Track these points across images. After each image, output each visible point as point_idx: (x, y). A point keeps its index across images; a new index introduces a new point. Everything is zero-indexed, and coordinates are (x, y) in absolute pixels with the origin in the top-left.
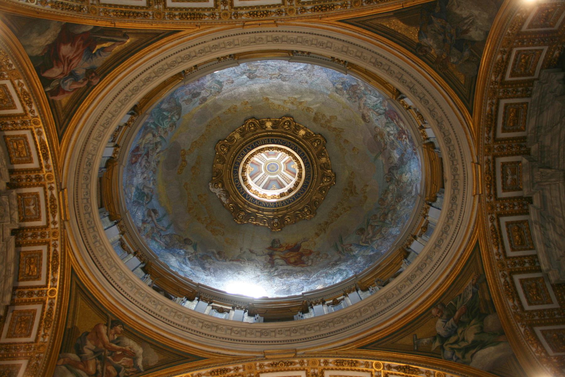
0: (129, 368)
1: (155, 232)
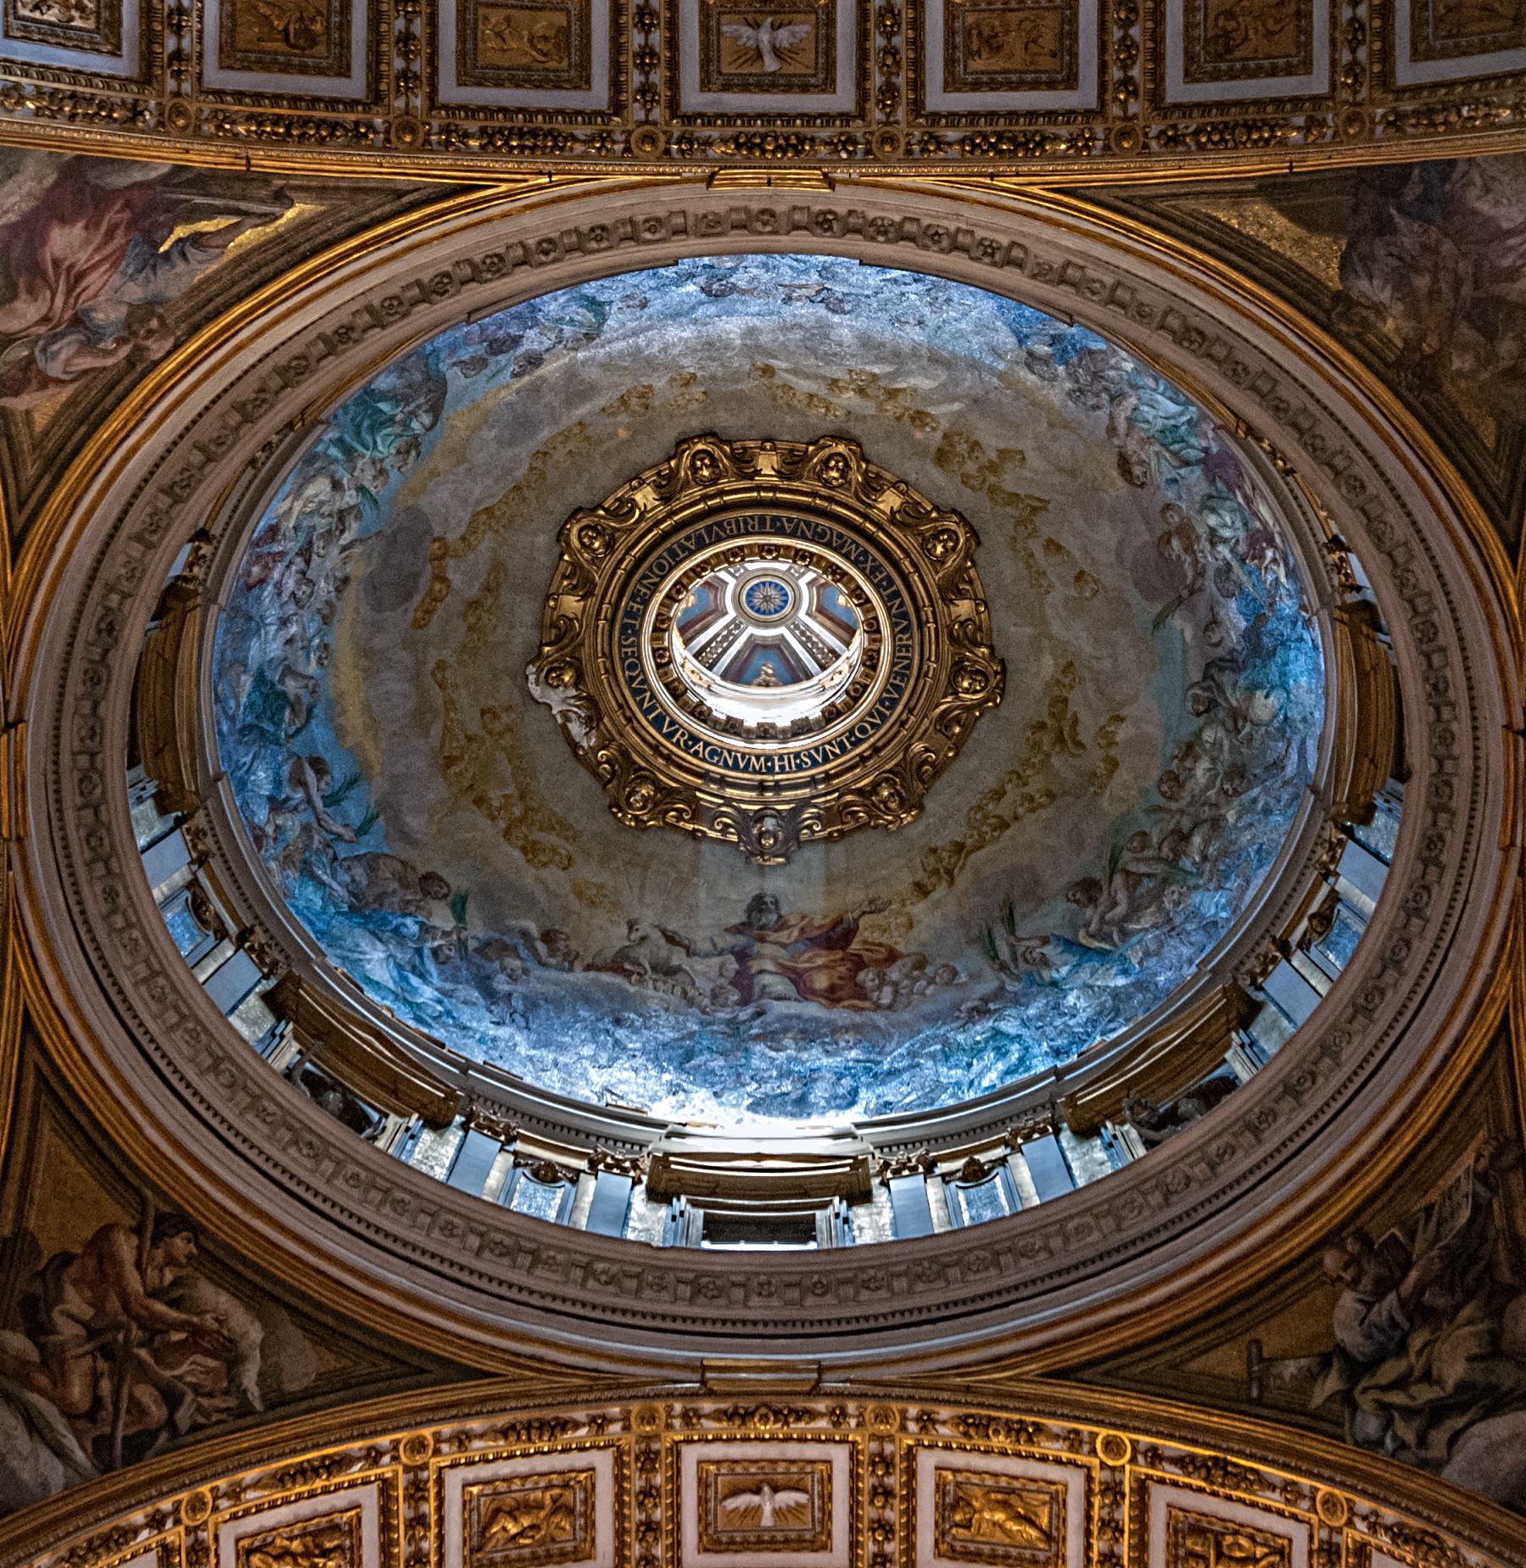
0: (210, 1395)
1: (316, 845)
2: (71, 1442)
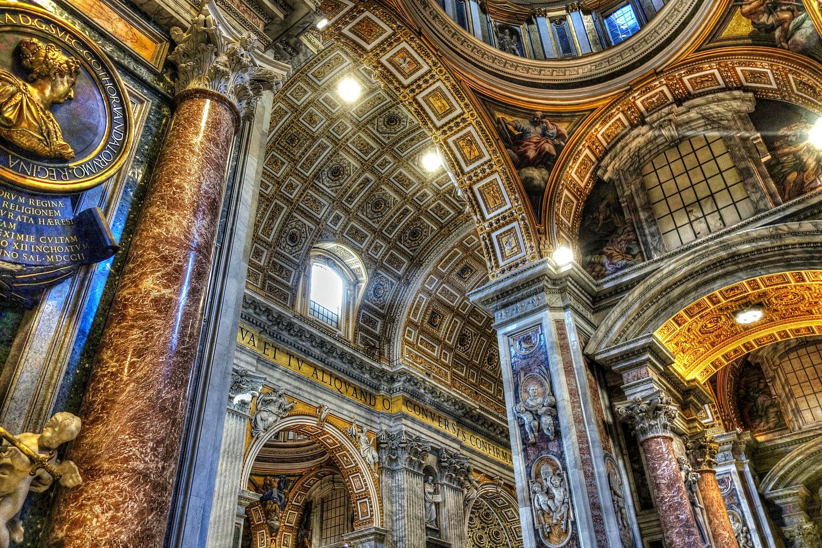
2: (800, 18)
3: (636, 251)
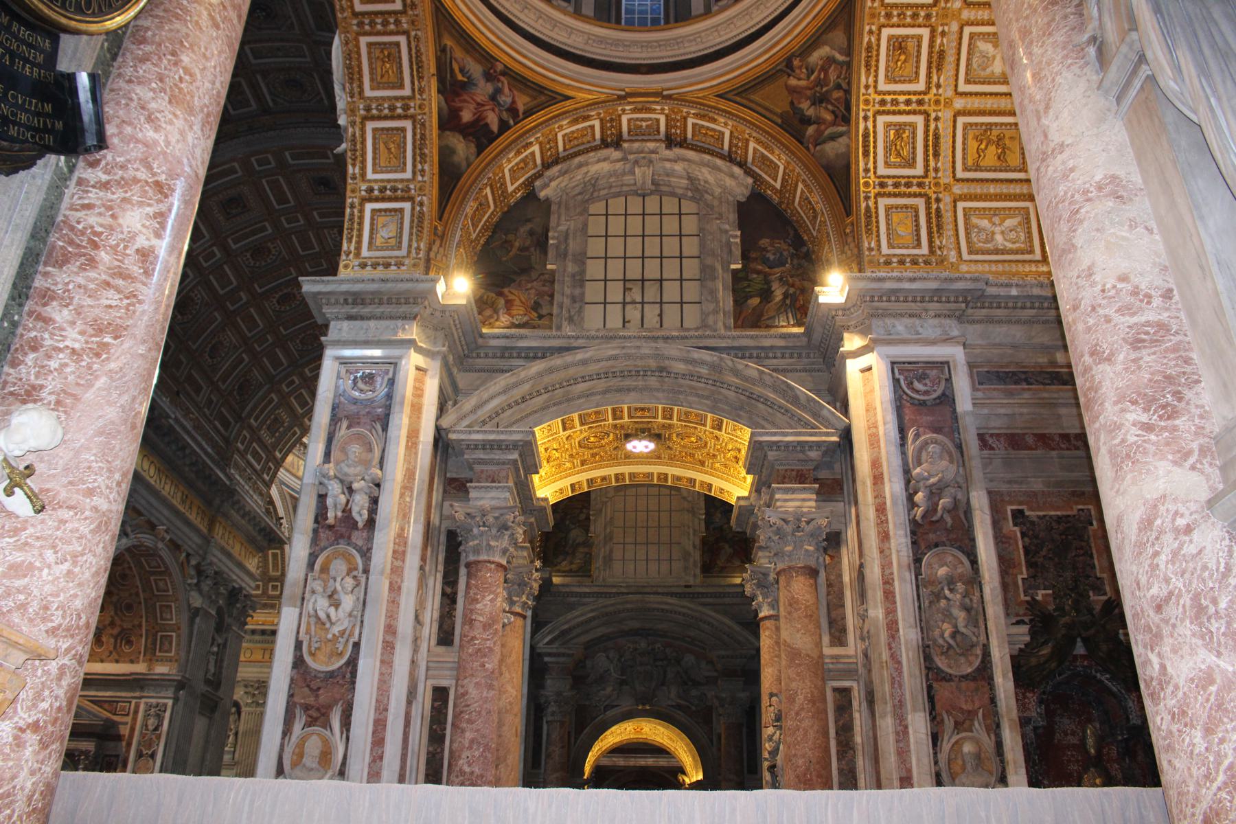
3: (544, 311)
